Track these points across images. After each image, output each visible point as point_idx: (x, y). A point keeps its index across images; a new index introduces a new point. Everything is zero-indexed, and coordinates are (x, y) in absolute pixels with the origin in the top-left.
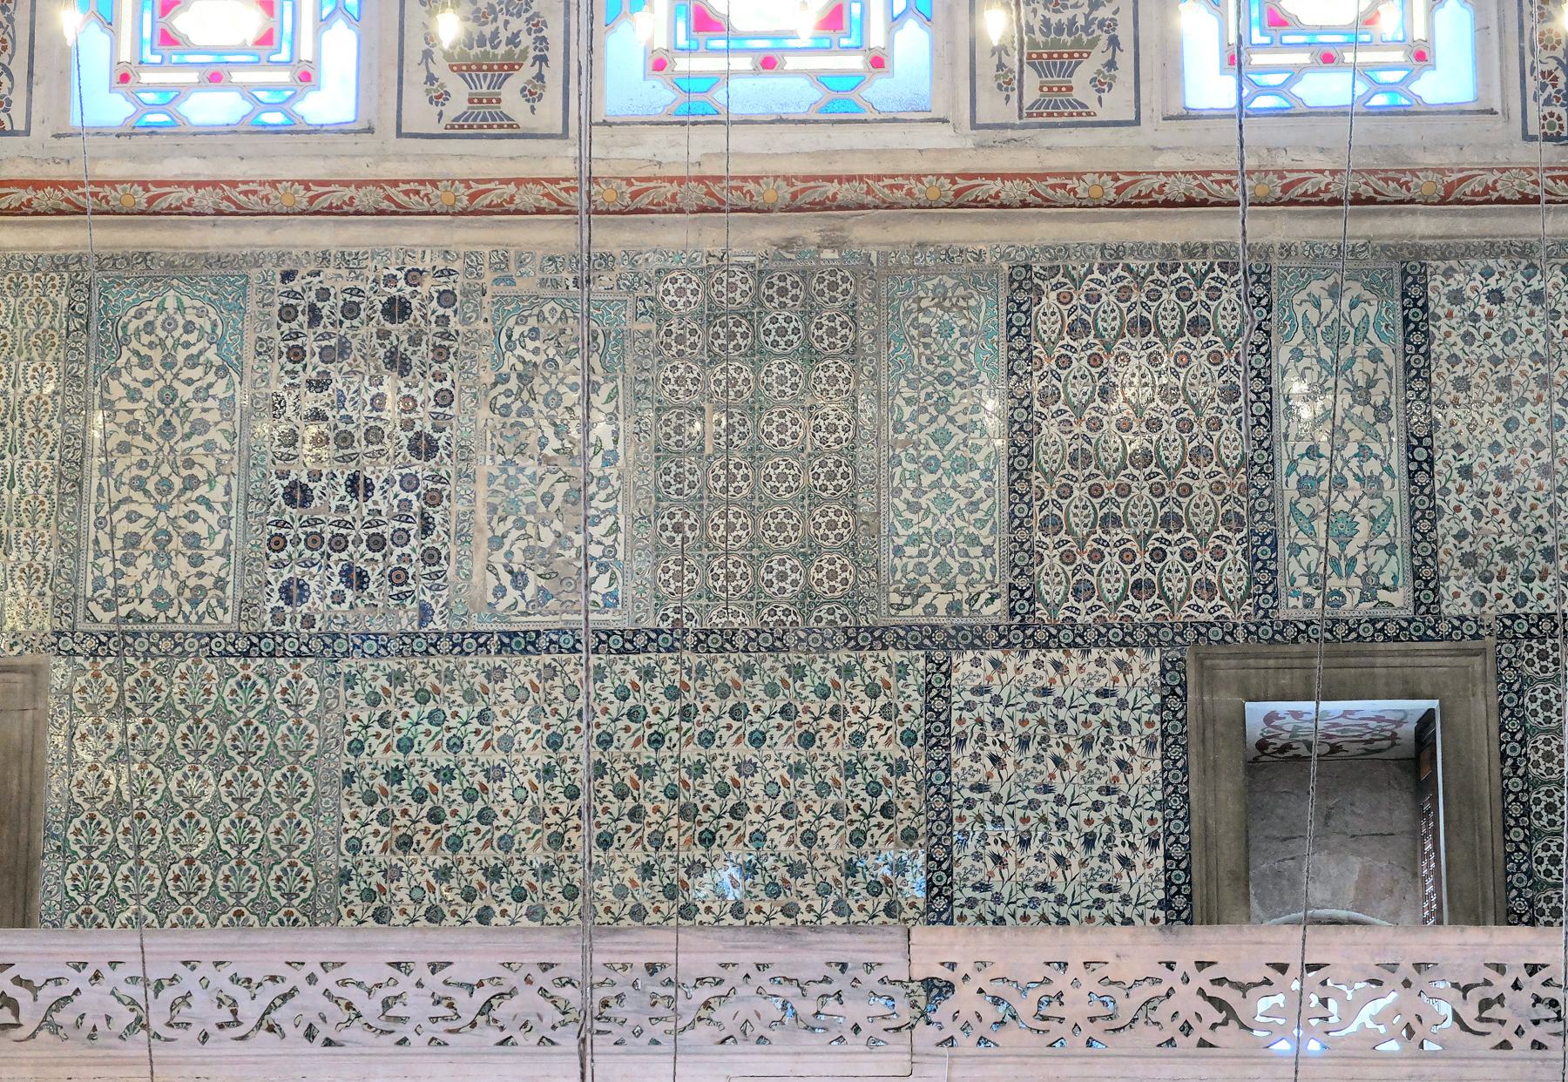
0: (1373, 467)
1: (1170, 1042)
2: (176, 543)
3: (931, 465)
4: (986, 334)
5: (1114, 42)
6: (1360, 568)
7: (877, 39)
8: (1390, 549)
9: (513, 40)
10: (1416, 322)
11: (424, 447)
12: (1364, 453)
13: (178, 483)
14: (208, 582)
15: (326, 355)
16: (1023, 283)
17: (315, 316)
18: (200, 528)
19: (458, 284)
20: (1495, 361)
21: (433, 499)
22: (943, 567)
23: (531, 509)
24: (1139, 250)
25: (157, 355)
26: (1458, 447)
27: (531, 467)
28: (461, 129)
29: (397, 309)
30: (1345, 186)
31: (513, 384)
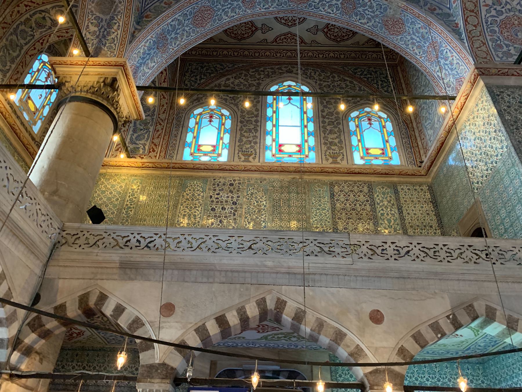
0: (393, 212)
1: (414, 260)
2: (192, 216)
3: (318, 209)
4: (326, 191)
5: (343, 155)
6: (393, 227)
7: (307, 153)
8: (398, 224)
9: (251, 152)
10: (396, 192)
11: (235, 203)
12: (391, 210)
13: (193, 207)
14: (197, 222)
15: (219, 190)
16: (332, 185)
17: (218, 185)
18: (196, 214)
19: (241, 182)
20: (410, 198)
21: (236, 211)
22: (321, 224)
23: (252, 213)
24: (350, 181)
25: (192, 189)
26: (407, 210)
27: (252, 207)
28: (243, 161)
29: (231, 185)
30: (384, 171)
31: (250, 195)
